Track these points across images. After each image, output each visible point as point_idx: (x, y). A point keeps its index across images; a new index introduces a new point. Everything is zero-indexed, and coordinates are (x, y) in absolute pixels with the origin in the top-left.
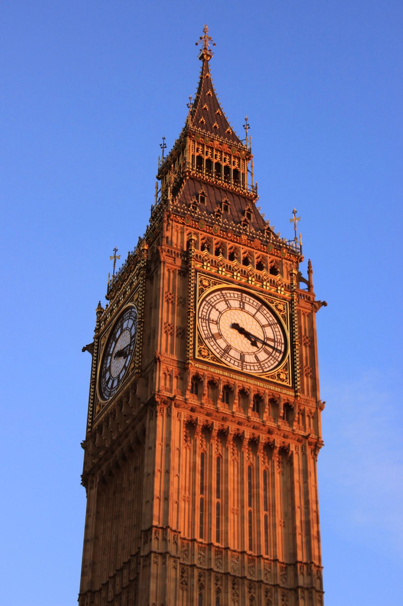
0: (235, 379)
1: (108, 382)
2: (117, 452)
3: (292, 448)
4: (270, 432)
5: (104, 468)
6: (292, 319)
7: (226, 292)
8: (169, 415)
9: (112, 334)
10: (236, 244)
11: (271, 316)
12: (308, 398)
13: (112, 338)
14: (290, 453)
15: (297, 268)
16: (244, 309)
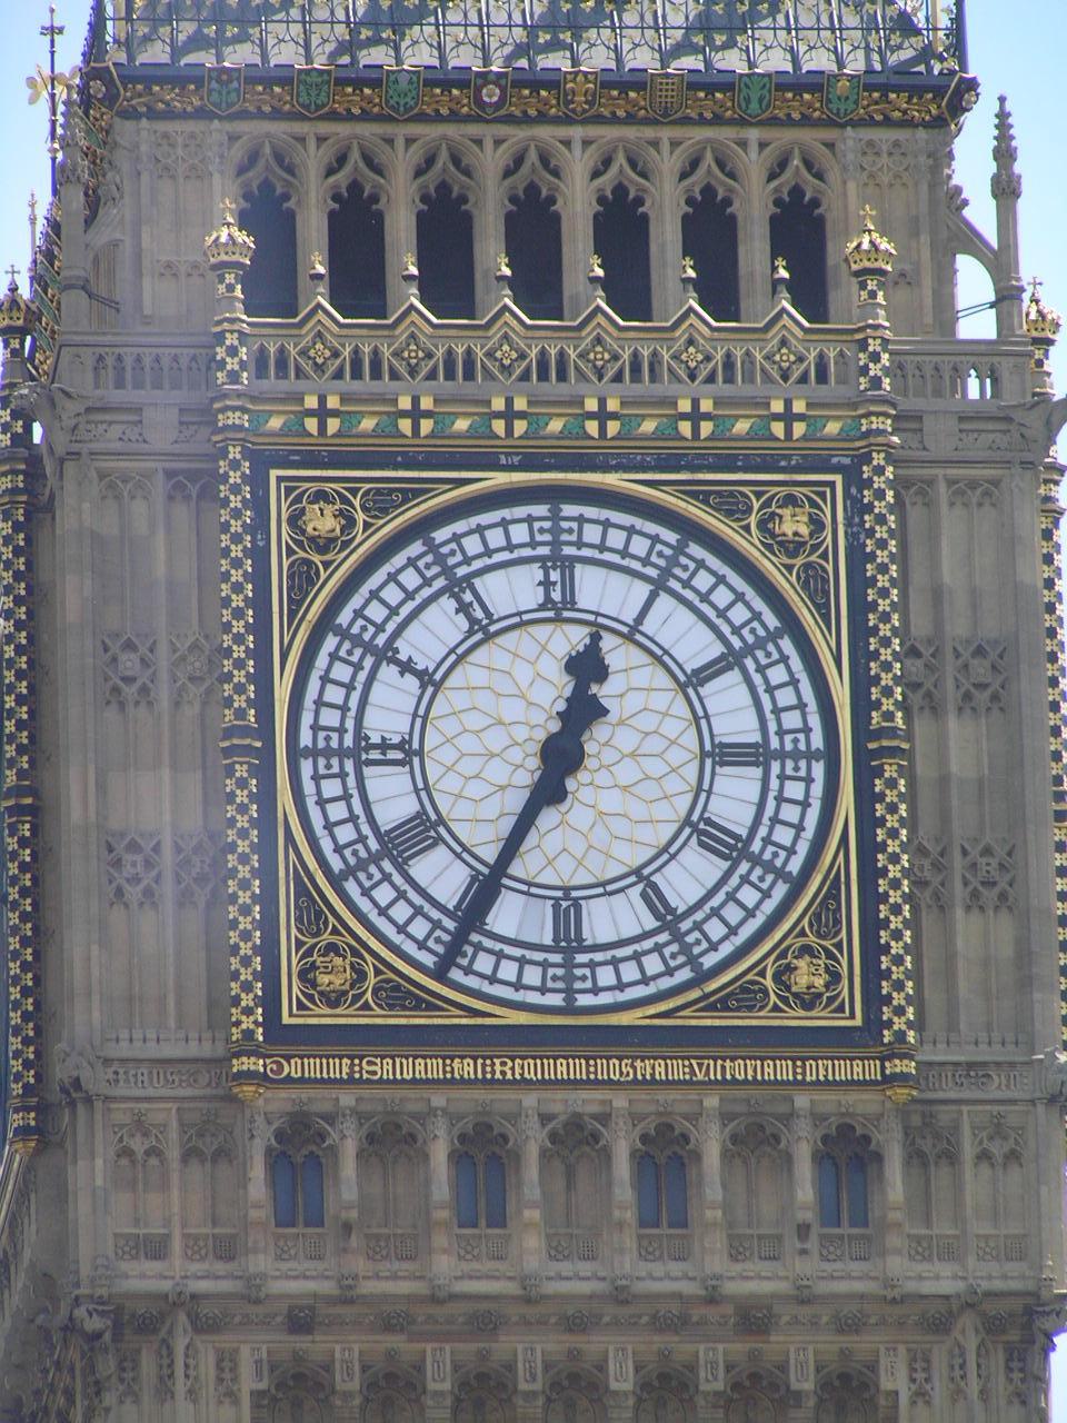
4: (754, 1319)
6: (859, 583)
7: (460, 526)
8: (165, 1390)
10: (545, 132)
11: (740, 597)
12: (983, 1054)
14: (882, 1402)
15: (942, 157)
16: (570, 602)
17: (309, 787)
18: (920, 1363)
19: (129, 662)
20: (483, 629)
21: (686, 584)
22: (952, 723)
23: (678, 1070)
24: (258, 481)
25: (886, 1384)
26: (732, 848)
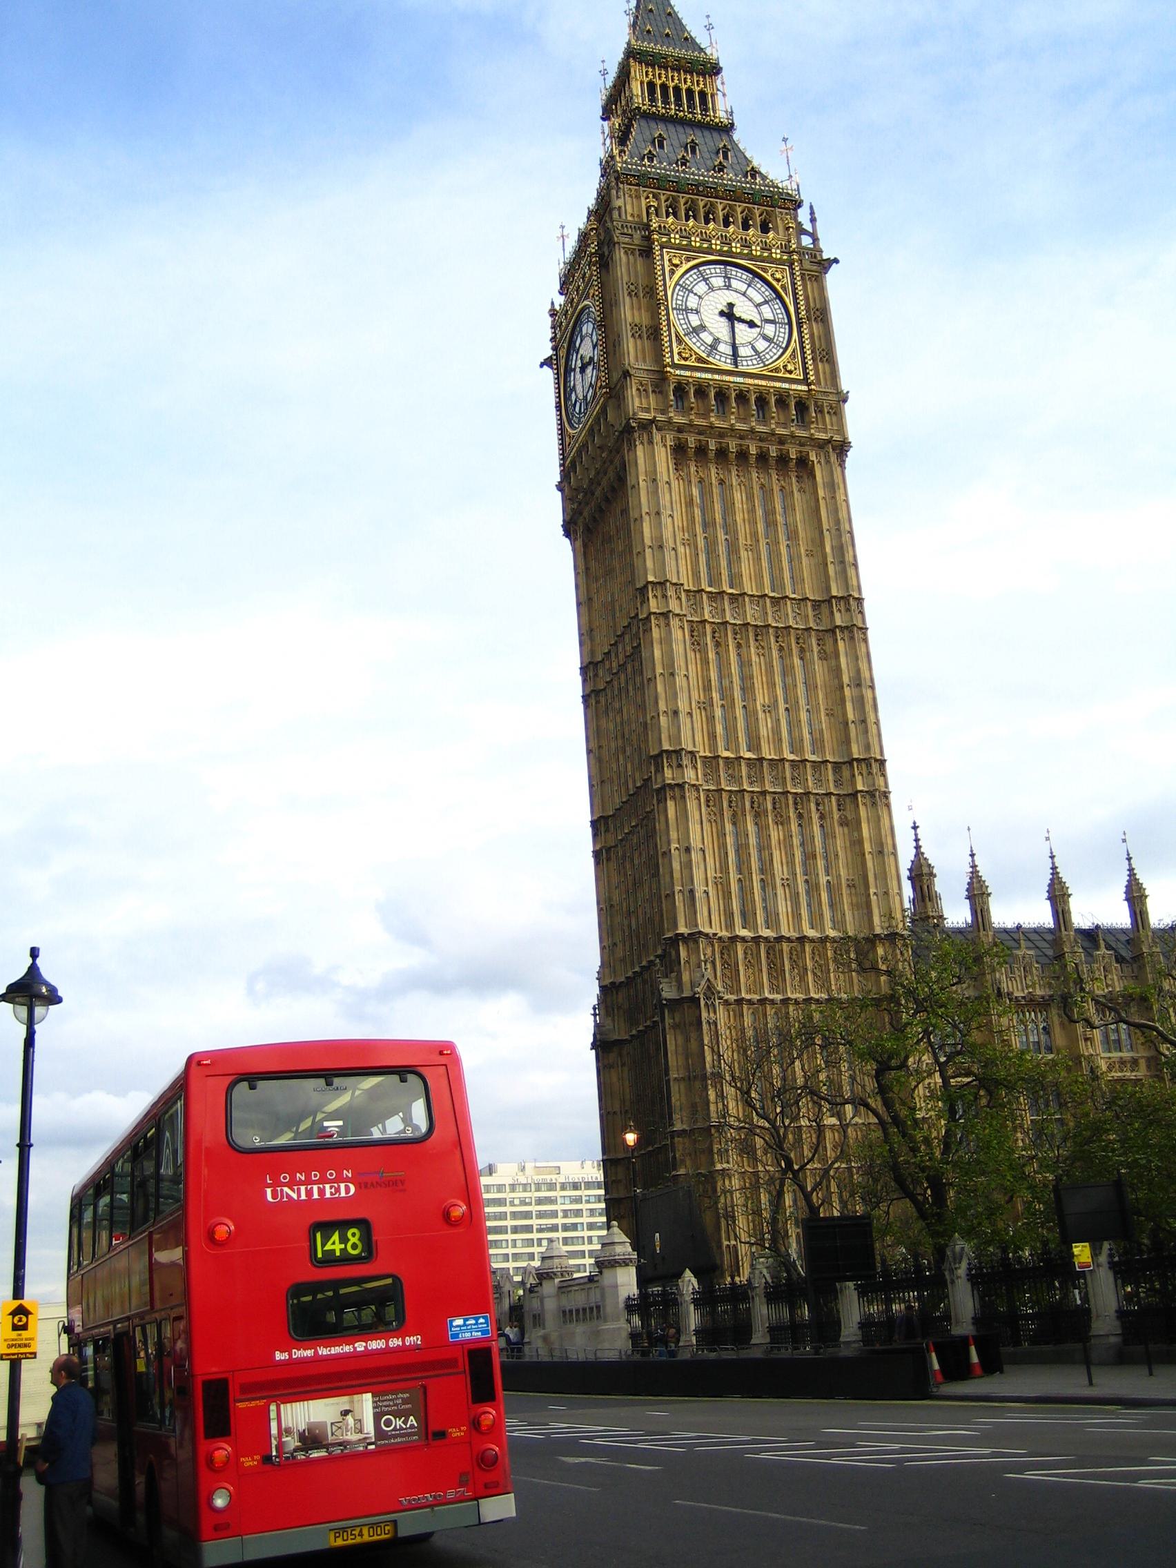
1: (575, 405)
2: (598, 493)
3: (813, 457)
4: (781, 441)
5: (586, 514)
6: (794, 289)
8: (651, 442)
9: (572, 342)
13: (572, 348)
19: (632, 287)
20: (711, 289)
23: (763, 383)
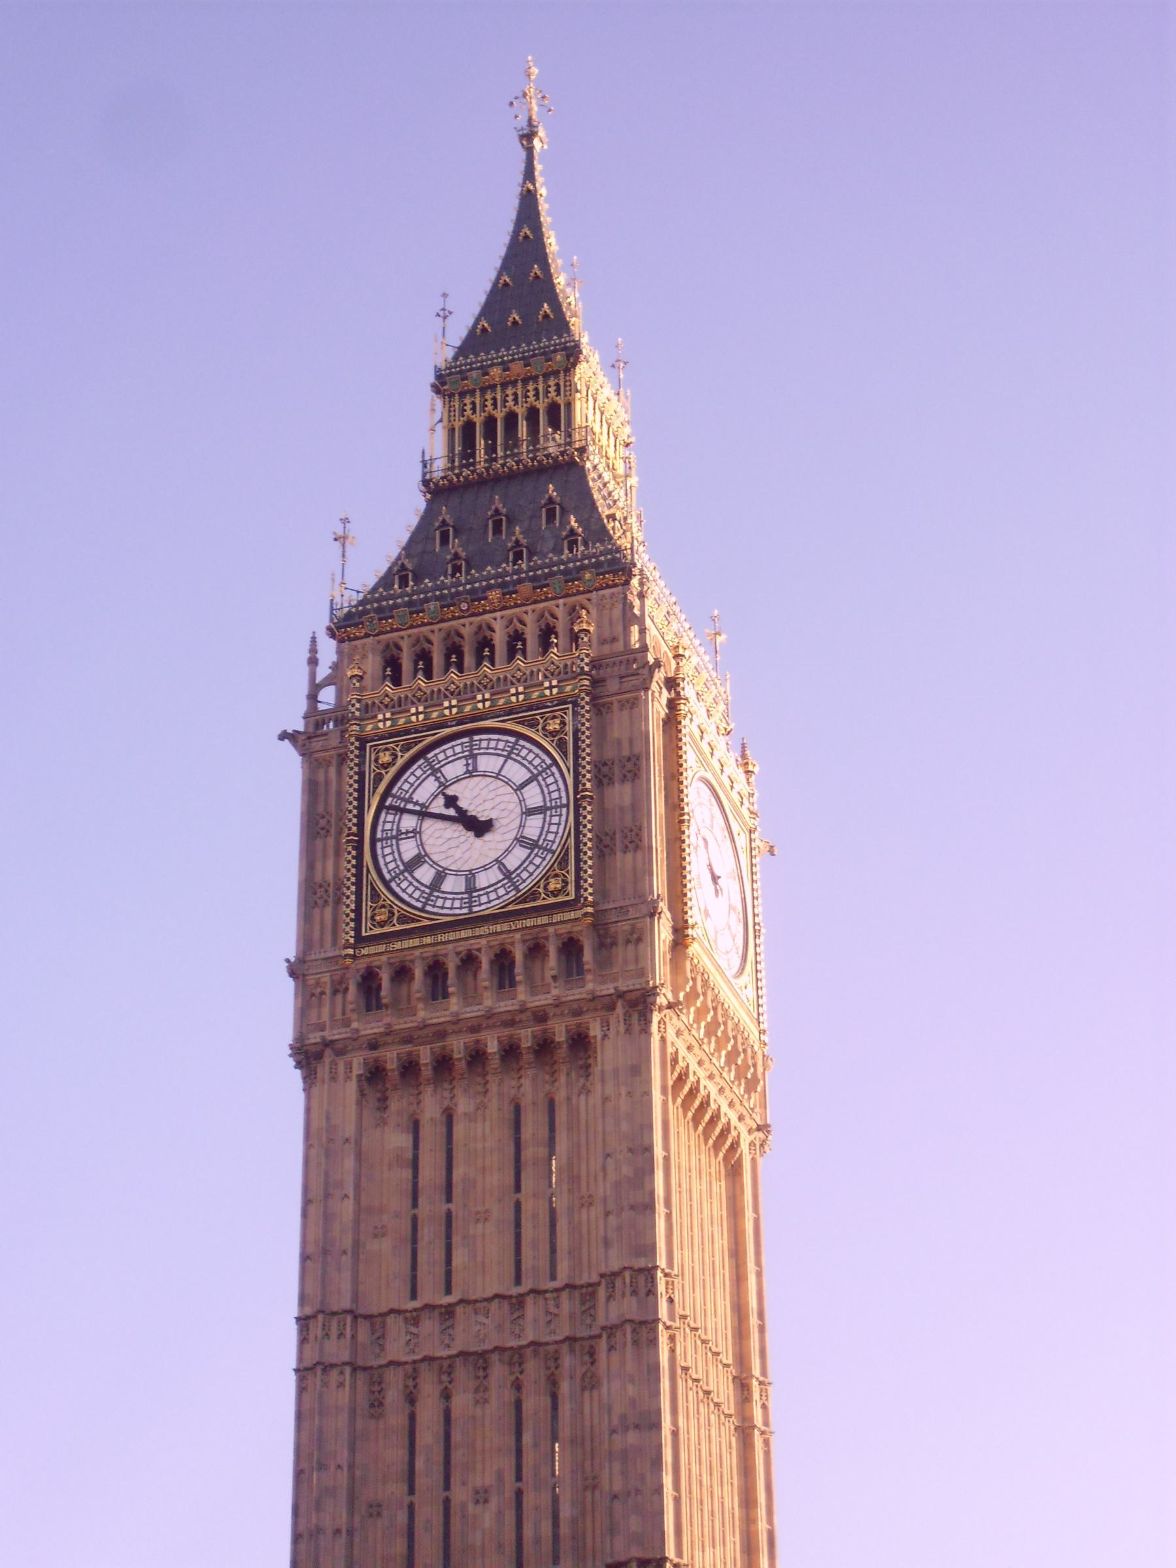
0: (449, 942)
3: (595, 1031)
4: (541, 1017)
6: (576, 739)
7: (437, 751)
10: (487, 617)
16: (475, 770)
17: (379, 852)
18: (606, 1024)
19: (323, 822)
21: (518, 755)
22: (617, 785)
23: (505, 927)
24: (362, 748)
25: (592, 1033)
26: (533, 845)
